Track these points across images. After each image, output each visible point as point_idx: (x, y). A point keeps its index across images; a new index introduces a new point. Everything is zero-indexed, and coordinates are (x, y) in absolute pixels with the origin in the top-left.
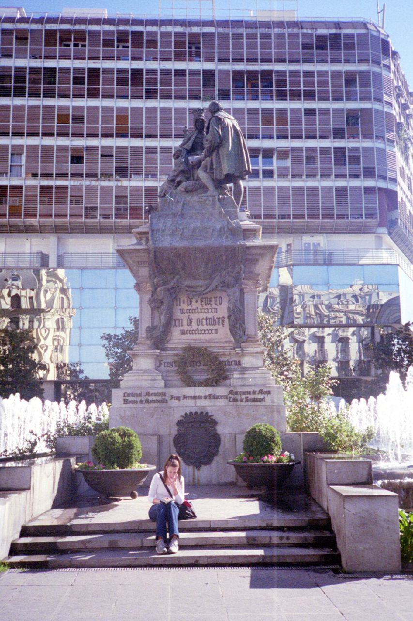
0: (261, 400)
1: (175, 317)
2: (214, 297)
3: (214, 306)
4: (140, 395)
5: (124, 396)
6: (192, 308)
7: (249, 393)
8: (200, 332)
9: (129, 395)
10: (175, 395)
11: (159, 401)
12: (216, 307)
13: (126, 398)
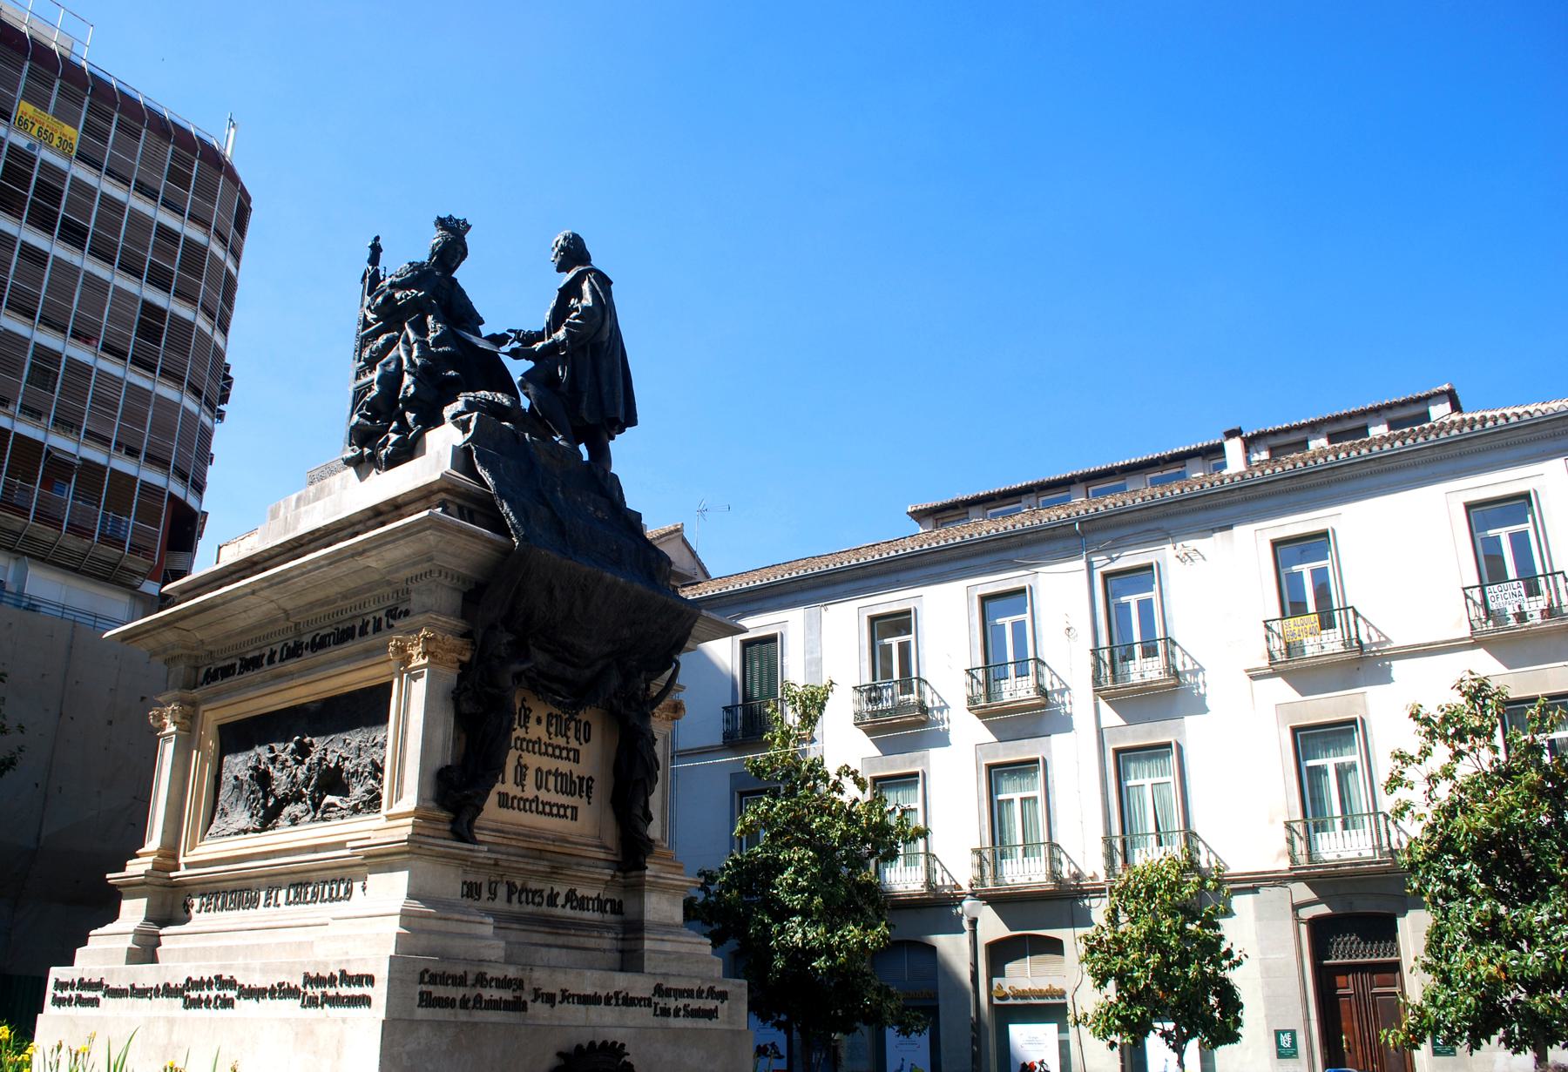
0: (711, 1014)
3: (574, 744)
4: (460, 981)
9: (435, 979)
10: (545, 990)
13: (425, 988)
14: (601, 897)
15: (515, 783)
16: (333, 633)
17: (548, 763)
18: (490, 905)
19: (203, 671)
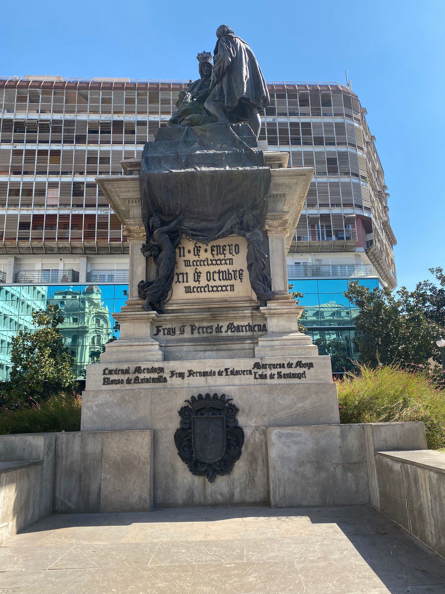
0: (299, 376)
1: (177, 271)
2: (229, 245)
3: (229, 256)
4: (127, 372)
5: (104, 373)
6: (200, 259)
7: (282, 366)
8: (210, 289)
9: (111, 372)
10: (178, 371)
11: (154, 380)
12: (230, 256)
13: (106, 376)
14: (251, 324)
15: (195, 281)
17: (212, 269)
18: (181, 336)
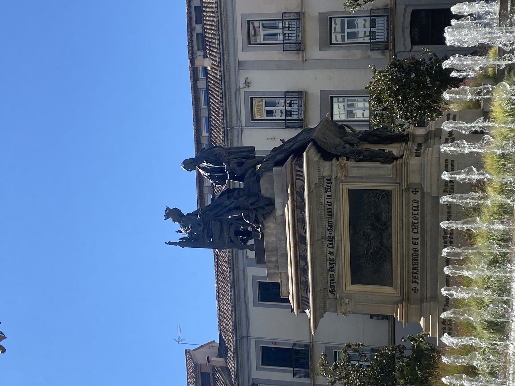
16: (328, 221)
19: (331, 296)
